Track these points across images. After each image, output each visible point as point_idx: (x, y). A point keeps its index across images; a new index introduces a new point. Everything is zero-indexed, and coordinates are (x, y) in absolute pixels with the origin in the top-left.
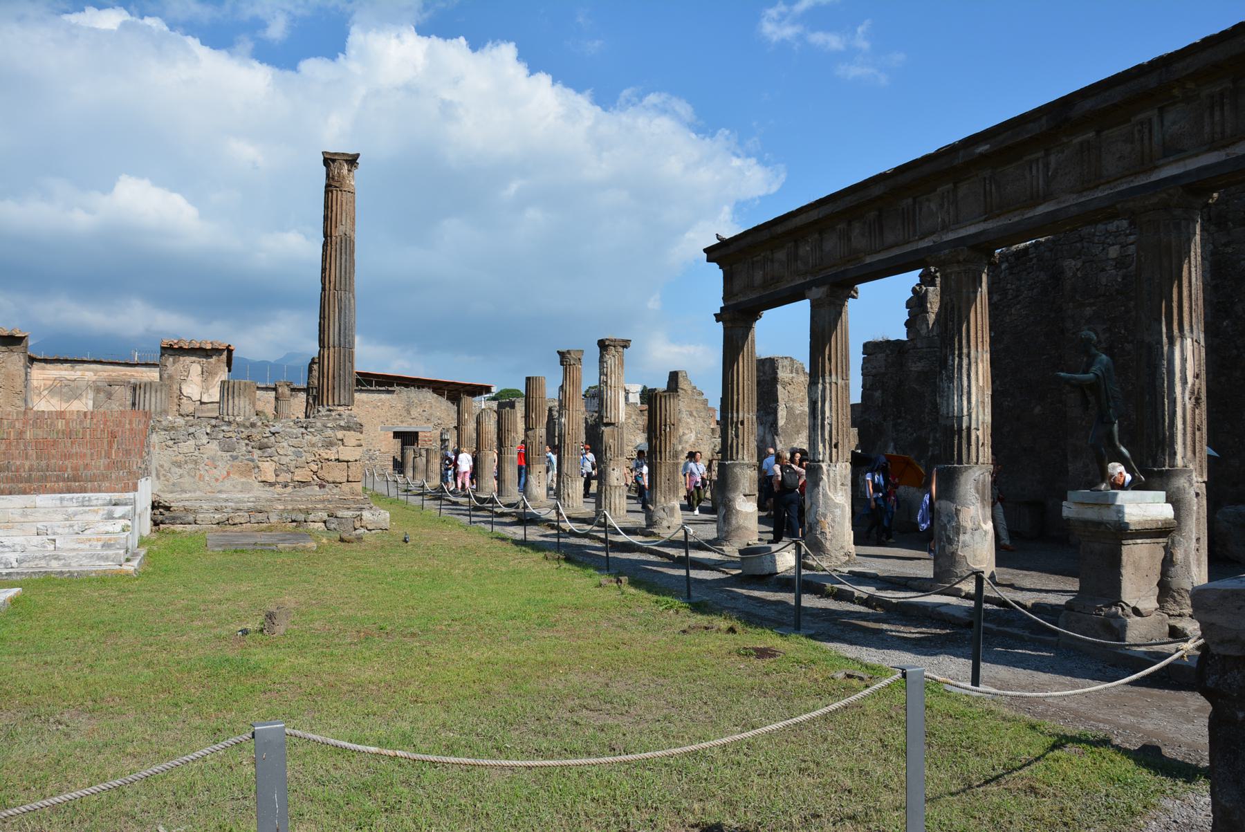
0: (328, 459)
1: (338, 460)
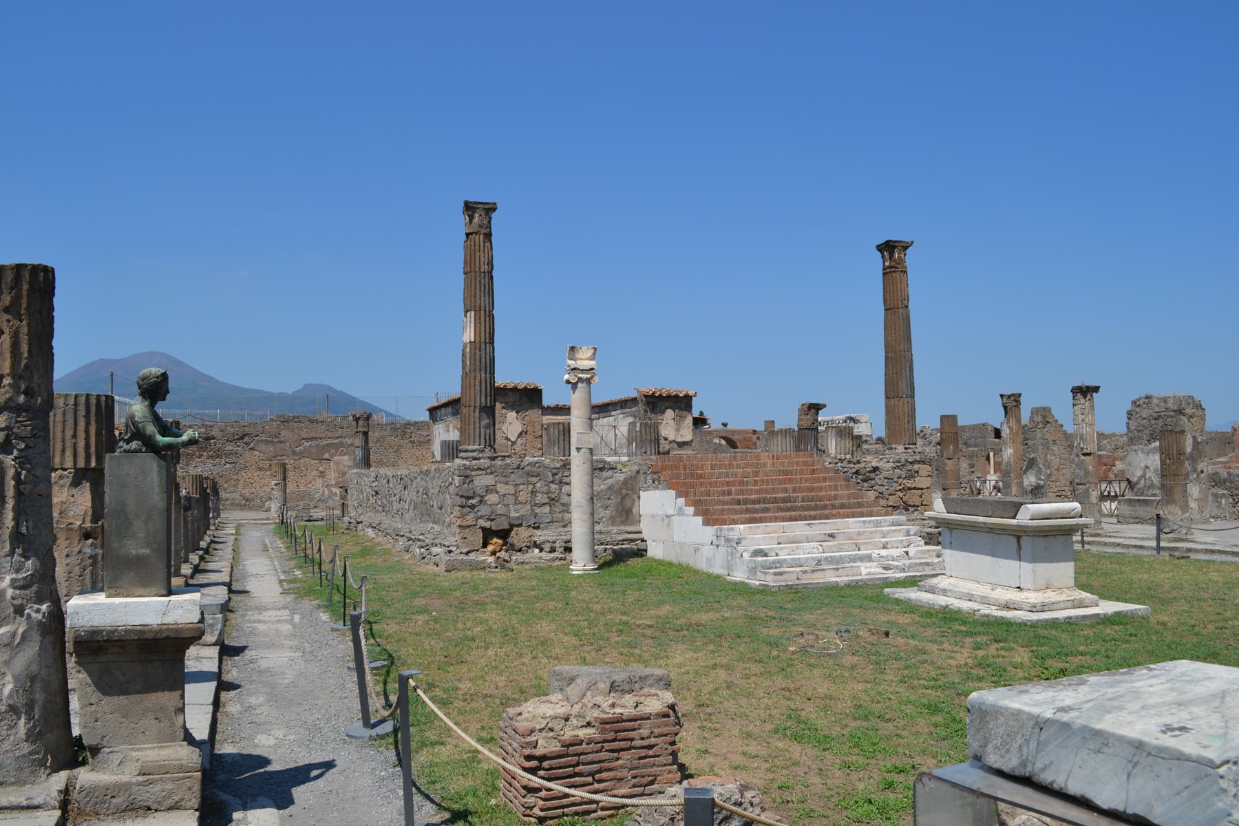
1: (915, 488)
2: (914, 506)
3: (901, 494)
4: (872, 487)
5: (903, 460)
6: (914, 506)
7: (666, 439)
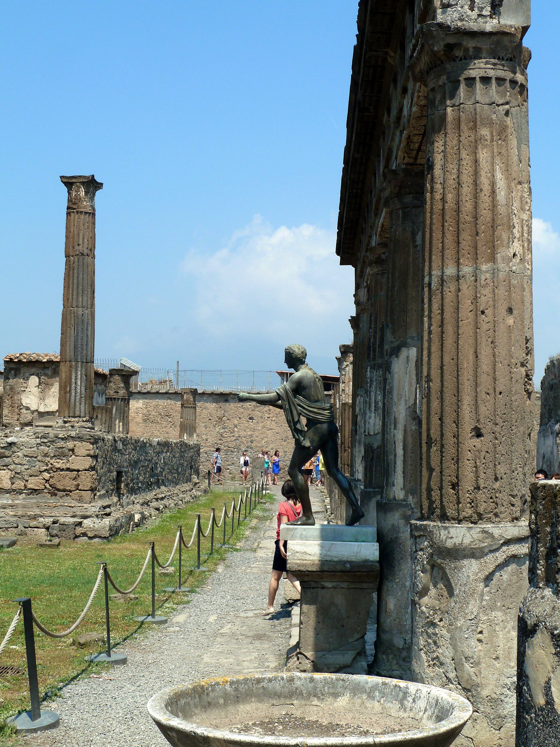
0: (59, 468)
1: (68, 469)
2: (64, 490)
3: (46, 475)
4: (7, 466)
5: (51, 435)
6: (64, 490)
7: (28, 408)
